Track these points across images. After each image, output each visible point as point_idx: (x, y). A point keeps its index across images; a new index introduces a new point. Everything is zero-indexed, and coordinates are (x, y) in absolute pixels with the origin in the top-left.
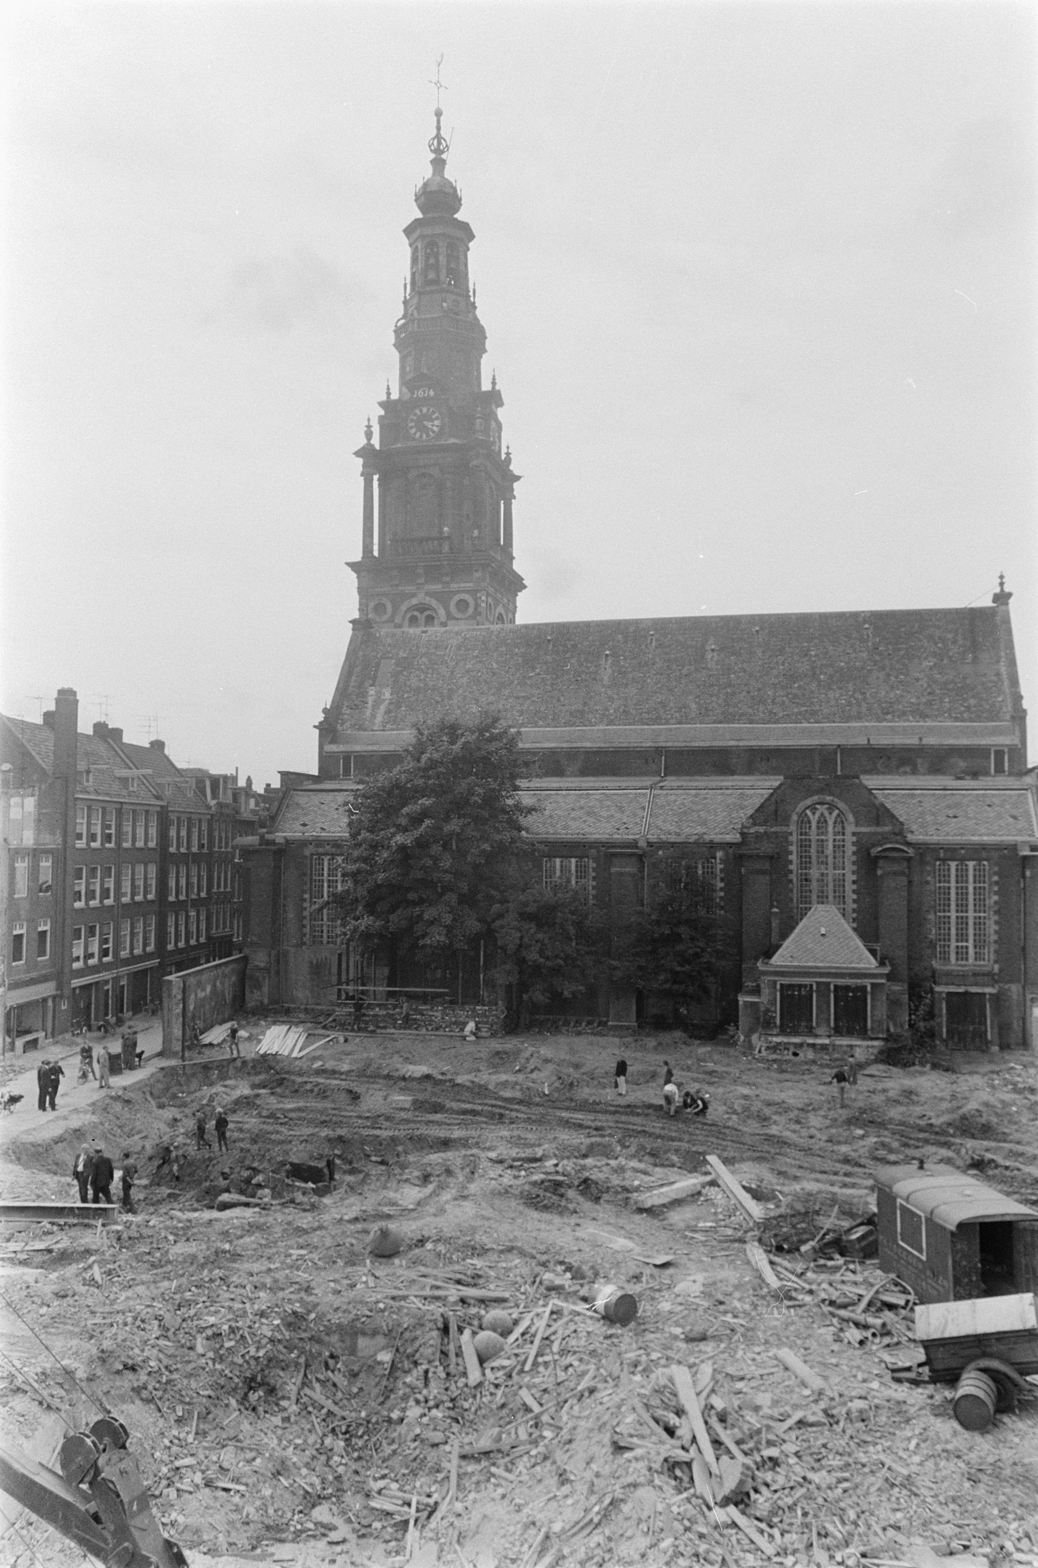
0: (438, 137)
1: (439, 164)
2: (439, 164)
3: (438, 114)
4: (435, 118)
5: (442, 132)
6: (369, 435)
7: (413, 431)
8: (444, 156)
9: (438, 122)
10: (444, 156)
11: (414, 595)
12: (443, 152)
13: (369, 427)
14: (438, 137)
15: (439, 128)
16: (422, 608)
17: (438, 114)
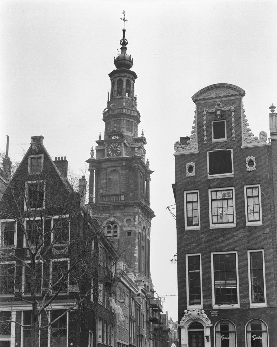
1: (124, 49)
2: (124, 49)
3: (124, 31)
4: (123, 32)
5: (126, 37)
6: (92, 155)
7: (110, 152)
8: (126, 46)
9: (124, 33)
10: (126, 46)
11: (109, 217)
12: (126, 45)
13: (92, 151)
15: (124, 36)
17: (124, 31)
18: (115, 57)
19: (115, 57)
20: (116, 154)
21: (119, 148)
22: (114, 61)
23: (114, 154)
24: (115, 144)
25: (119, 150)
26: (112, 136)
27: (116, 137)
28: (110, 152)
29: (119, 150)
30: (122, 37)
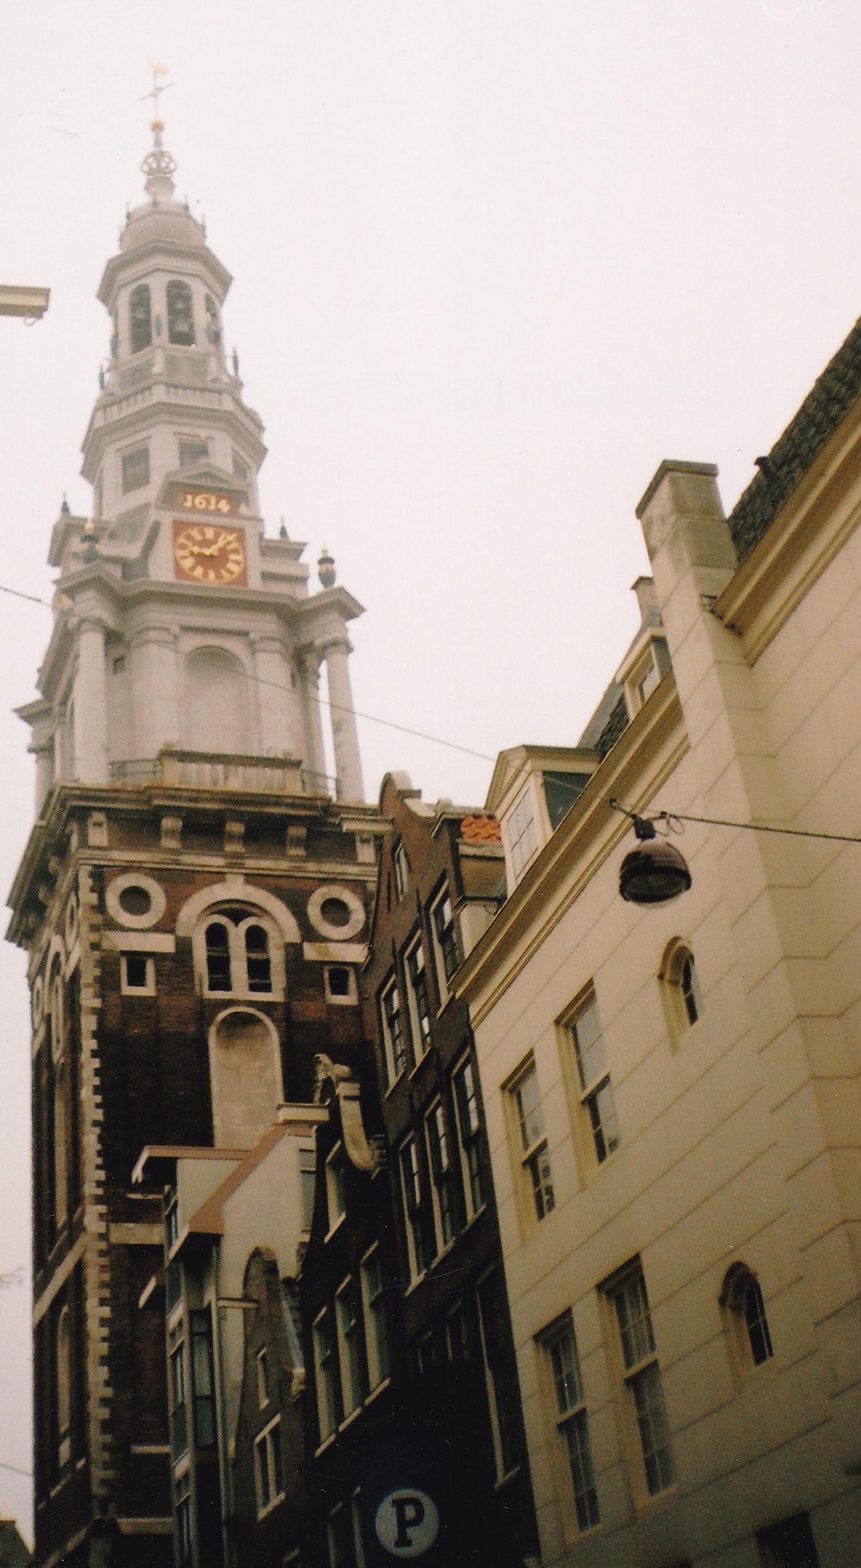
0: (159, 155)
3: (157, 127)
11: (218, 877)
14: (159, 155)
15: (158, 143)
16: (237, 911)
17: (157, 127)
18: (128, 204)
19: (128, 204)
20: (219, 576)
21: (236, 551)
22: (129, 216)
23: (212, 575)
24: (210, 533)
25: (237, 563)
26: (196, 490)
27: (217, 503)
28: (188, 563)
29: (237, 563)
30: (151, 148)
